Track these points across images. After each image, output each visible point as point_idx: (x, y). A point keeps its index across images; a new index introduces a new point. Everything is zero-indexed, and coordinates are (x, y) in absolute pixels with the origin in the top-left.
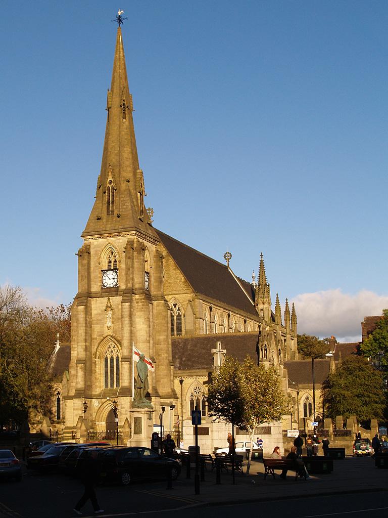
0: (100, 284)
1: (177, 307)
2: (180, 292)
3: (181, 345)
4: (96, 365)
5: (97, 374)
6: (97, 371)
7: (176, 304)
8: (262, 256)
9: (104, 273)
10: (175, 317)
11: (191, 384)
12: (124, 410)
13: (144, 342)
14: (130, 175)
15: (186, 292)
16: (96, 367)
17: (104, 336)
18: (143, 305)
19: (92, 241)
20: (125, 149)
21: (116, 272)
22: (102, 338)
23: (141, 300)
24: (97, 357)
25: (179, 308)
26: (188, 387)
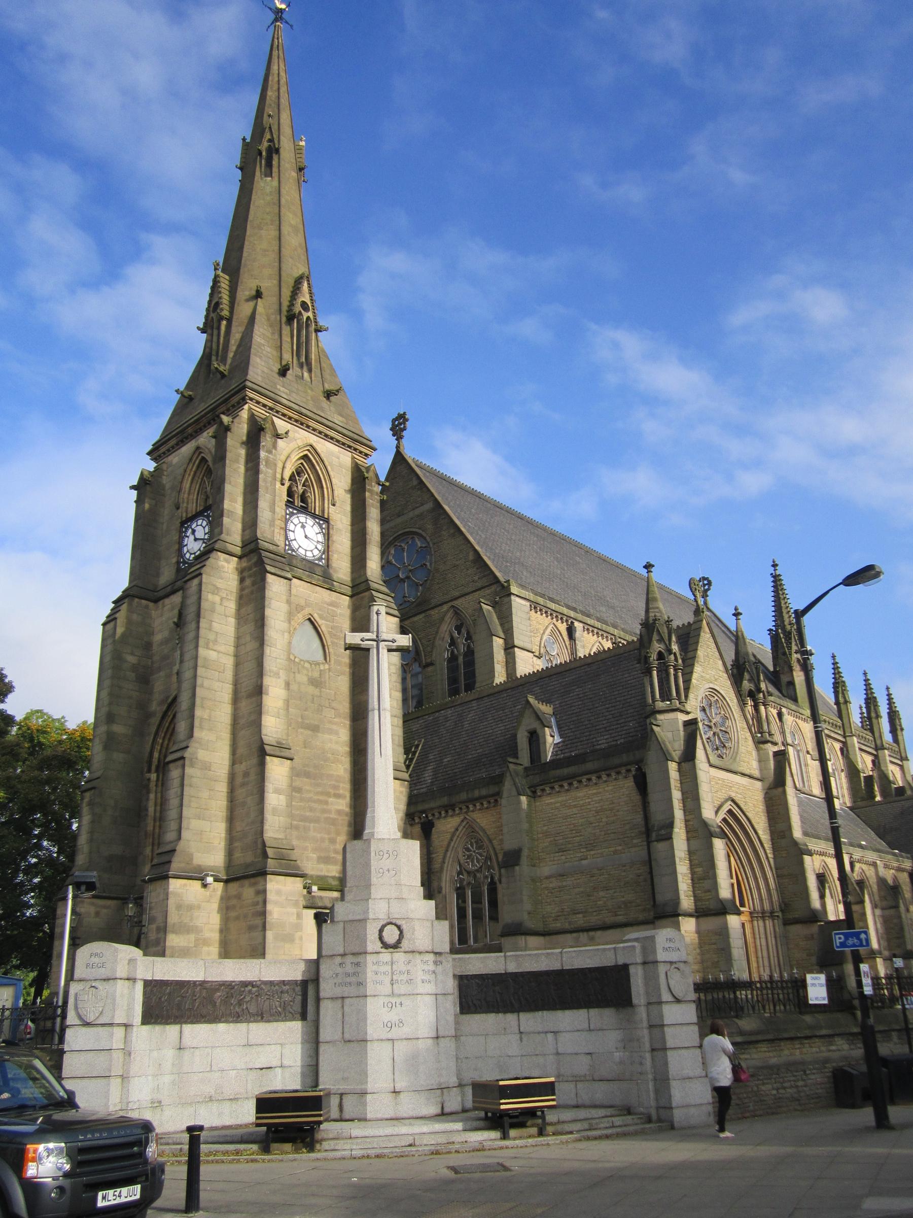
0: (174, 560)
1: (464, 631)
2: (467, 590)
3: (448, 724)
4: (148, 792)
5: (150, 821)
6: (151, 809)
7: (462, 625)
8: (775, 565)
9: (187, 529)
10: (461, 659)
11: (453, 835)
12: (154, 927)
13: (250, 696)
14: (268, 285)
15: (479, 585)
16: (148, 799)
17: (170, 700)
18: (254, 584)
19: (170, 458)
20: (263, 232)
21: (208, 517)
22: (165, 708)
23: (250, 569)
24: (153, 768)
25: (468, 633)
26: (446, 843)
